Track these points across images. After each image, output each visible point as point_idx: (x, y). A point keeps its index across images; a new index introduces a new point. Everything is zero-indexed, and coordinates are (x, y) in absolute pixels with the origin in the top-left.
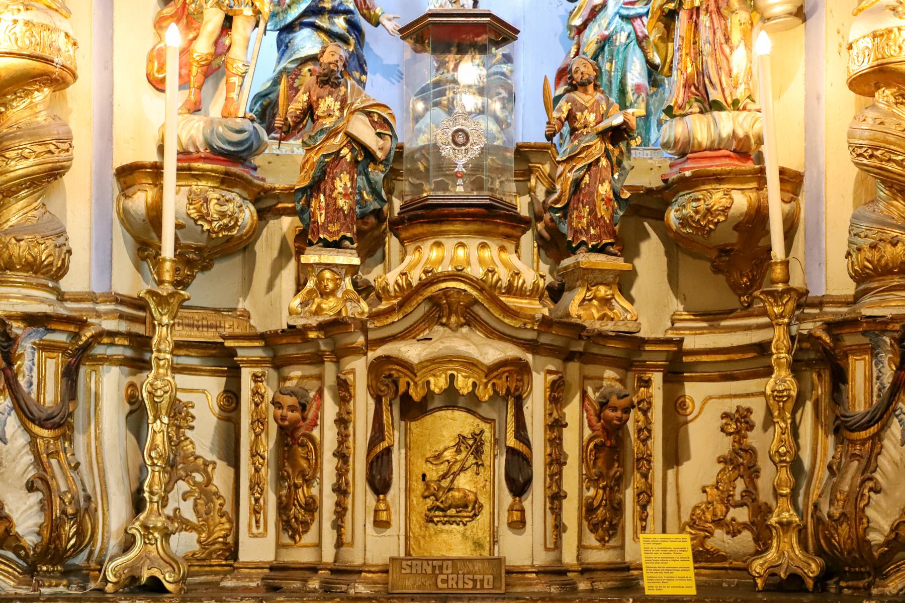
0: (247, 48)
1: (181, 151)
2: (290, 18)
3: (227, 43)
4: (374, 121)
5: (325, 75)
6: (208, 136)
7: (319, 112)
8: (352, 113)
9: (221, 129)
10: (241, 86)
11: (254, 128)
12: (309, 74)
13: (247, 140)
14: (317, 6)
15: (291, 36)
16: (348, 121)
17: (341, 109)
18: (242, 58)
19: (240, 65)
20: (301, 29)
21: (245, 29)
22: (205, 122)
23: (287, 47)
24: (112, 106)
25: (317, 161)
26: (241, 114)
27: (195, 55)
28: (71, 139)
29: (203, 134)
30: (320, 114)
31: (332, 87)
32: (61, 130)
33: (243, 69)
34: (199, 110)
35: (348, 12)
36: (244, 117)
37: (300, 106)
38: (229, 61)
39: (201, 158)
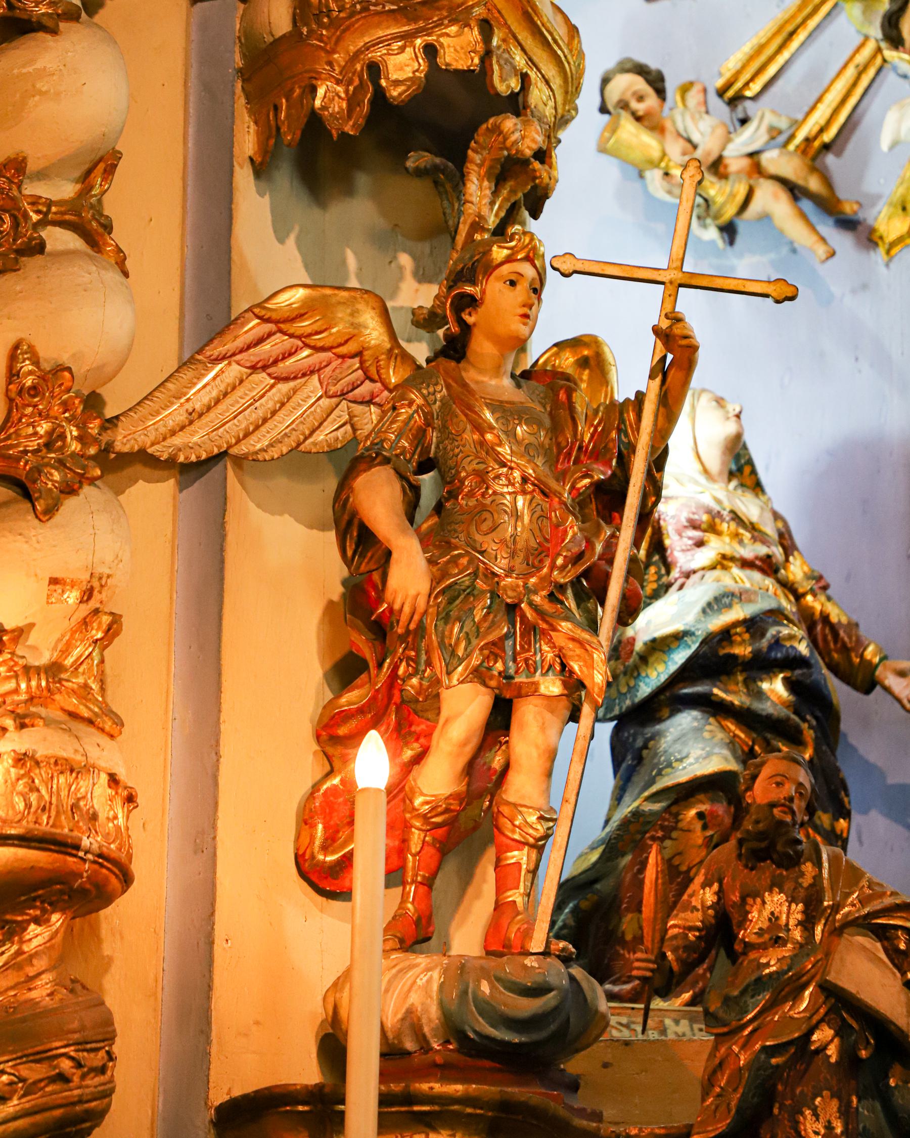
0: (549, 774)
1: (385, 1050)
2: (645, 689)
3: (497, 762)
4: (897, 950)
5: (761, 836)
6: (454, 1007)
7: (748, 934)
8: (836, 932)
9: (485, 987)
10: (534, 872)
11: (572, 978)
12: (698, 825)
13: (556, 1009)
14: (715, 654)
15: (649, 731)
16: (828, 954)
17: (807, 924)
18: (540, 802)
19: (532, 819)
20: (674, 712)
21: (543, 728)
22: (445, 971)
23: (639, 759)
24: (211, 943)
25: (750, 1065)
26: (537, 944)
27: (418, 802)
28: (111, 1038)
29: (441, 1004)
30: (752, 939)
31: (779, 866)
32: (90, 1017)
33: (541, 828)
34: (427, 939)
35: (794, 662)
36: (546, 953)
37: (696, 919)
38: (505, 810)
39: (436, 1065)
